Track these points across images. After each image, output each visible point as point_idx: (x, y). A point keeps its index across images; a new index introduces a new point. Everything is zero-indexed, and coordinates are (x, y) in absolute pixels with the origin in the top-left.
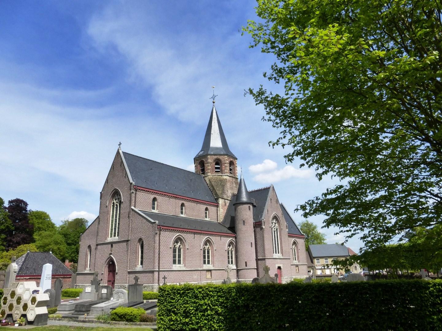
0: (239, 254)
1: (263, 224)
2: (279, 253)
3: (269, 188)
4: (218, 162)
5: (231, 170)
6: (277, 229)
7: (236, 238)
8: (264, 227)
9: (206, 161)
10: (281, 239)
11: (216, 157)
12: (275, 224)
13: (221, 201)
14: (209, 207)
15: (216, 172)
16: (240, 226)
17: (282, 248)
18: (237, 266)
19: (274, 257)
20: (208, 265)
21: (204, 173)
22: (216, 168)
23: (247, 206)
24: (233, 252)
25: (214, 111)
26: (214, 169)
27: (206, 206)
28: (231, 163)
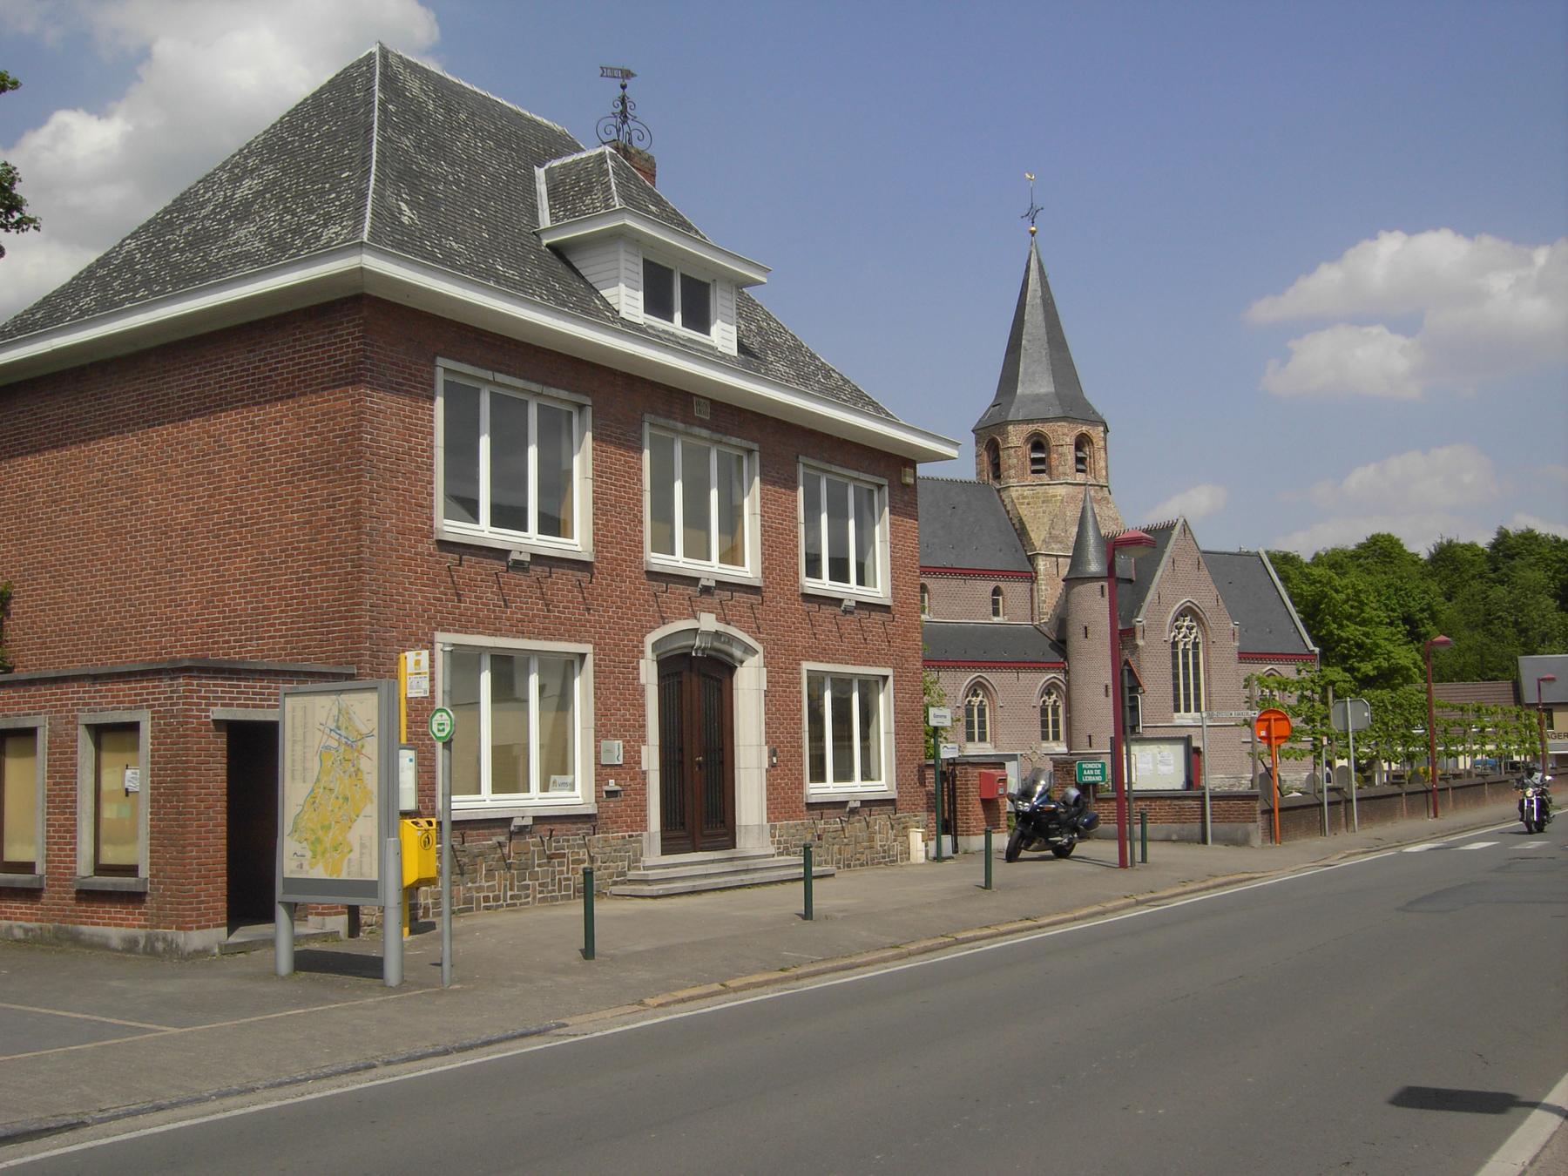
0: (1075, 714)
1: (1139, 634)
2: (1198, 709)
3: (1167, 529)
4: (1038, 443)
5: (1080, 460)
6: (1195, 645)
7: (1067, 673)
8: (1140, 642)
9: (1005, 440)
10: (1207, 671)
11: (1031, 428)
12: (1190, 628)
13: (1042, 565)
14: (1002, 585)
15: (1034, 472)
16: (1076, 641)
17: (1209, 695)
18: (1070, 747)
19: (1178, 722)
20: (982, 745)
21: (997, 477)
22: (1034, 461)
23: (1096, 586)
24: (1061, 710)
25: (1034, 274)
26: (1029, 462)
27: (993, 584)
28: (1082, 442)
